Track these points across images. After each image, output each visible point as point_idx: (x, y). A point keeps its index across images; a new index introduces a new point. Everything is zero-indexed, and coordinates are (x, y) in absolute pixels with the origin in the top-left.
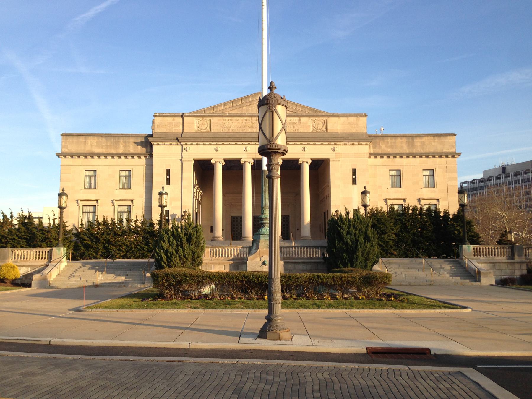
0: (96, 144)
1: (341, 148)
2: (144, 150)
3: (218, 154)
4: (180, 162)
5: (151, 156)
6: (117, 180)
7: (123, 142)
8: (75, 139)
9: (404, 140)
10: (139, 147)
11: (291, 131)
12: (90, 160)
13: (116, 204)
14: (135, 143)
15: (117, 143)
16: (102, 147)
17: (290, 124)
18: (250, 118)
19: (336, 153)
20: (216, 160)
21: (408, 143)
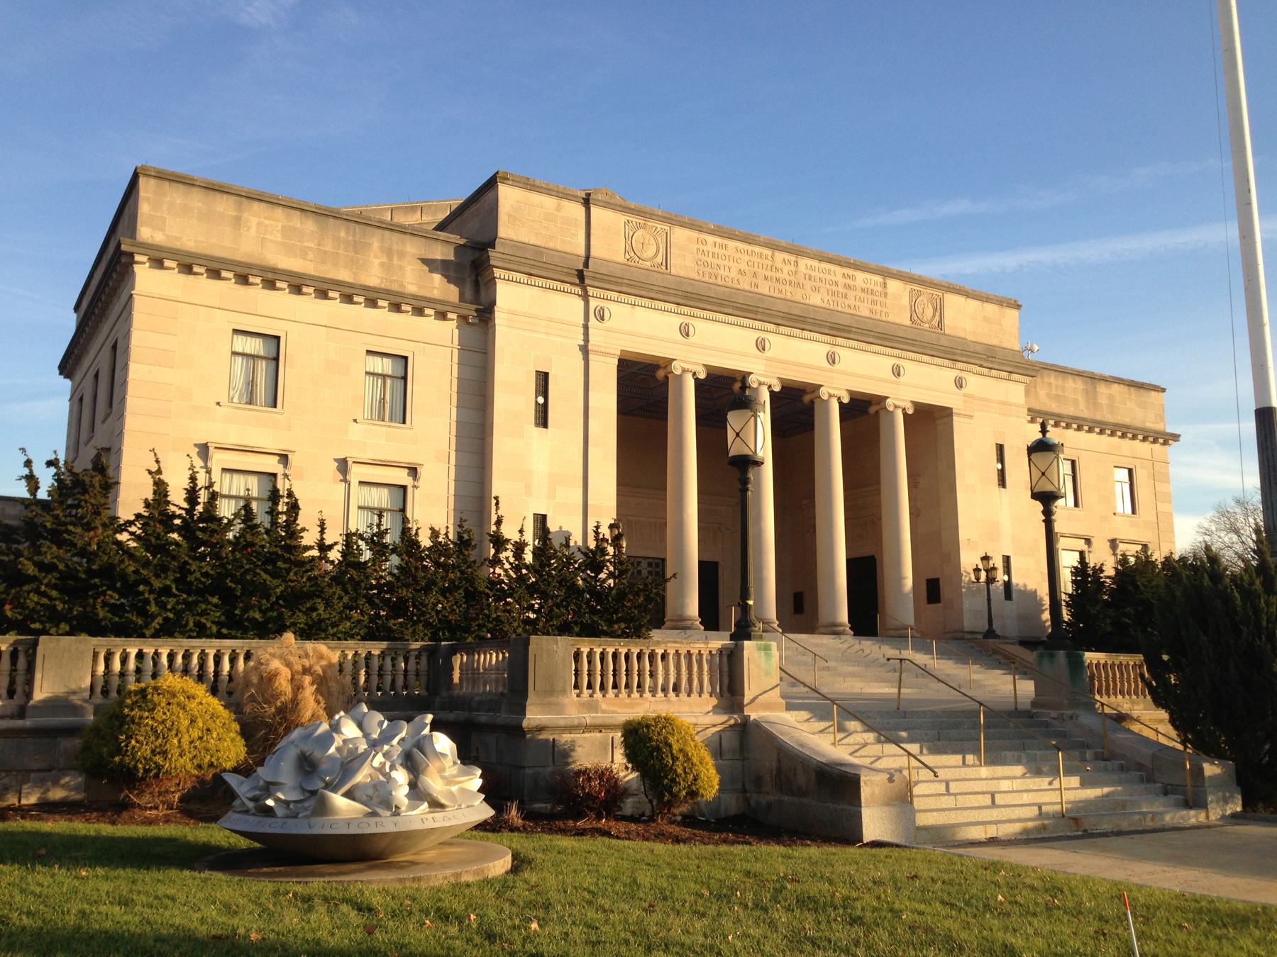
0: (279, 237)
1: (978, 383)
2: (451, 293)
3: (700, 347)
4: (580, 356)
5: (485, 313)
6: (358, 387)
7: (381, 248)
8: (197, 200)
9: (1079, 384)
10: (437, 278)
11: (866, 313)
12: (256, 294)
13: (356, 473)
14: (425, 261)
15: (359, 248)
16: (303, 254)
17: (863, 291)
18: (768, 252)
19: (965, 395)
20: (686, 366)
21: (1086, 391)
